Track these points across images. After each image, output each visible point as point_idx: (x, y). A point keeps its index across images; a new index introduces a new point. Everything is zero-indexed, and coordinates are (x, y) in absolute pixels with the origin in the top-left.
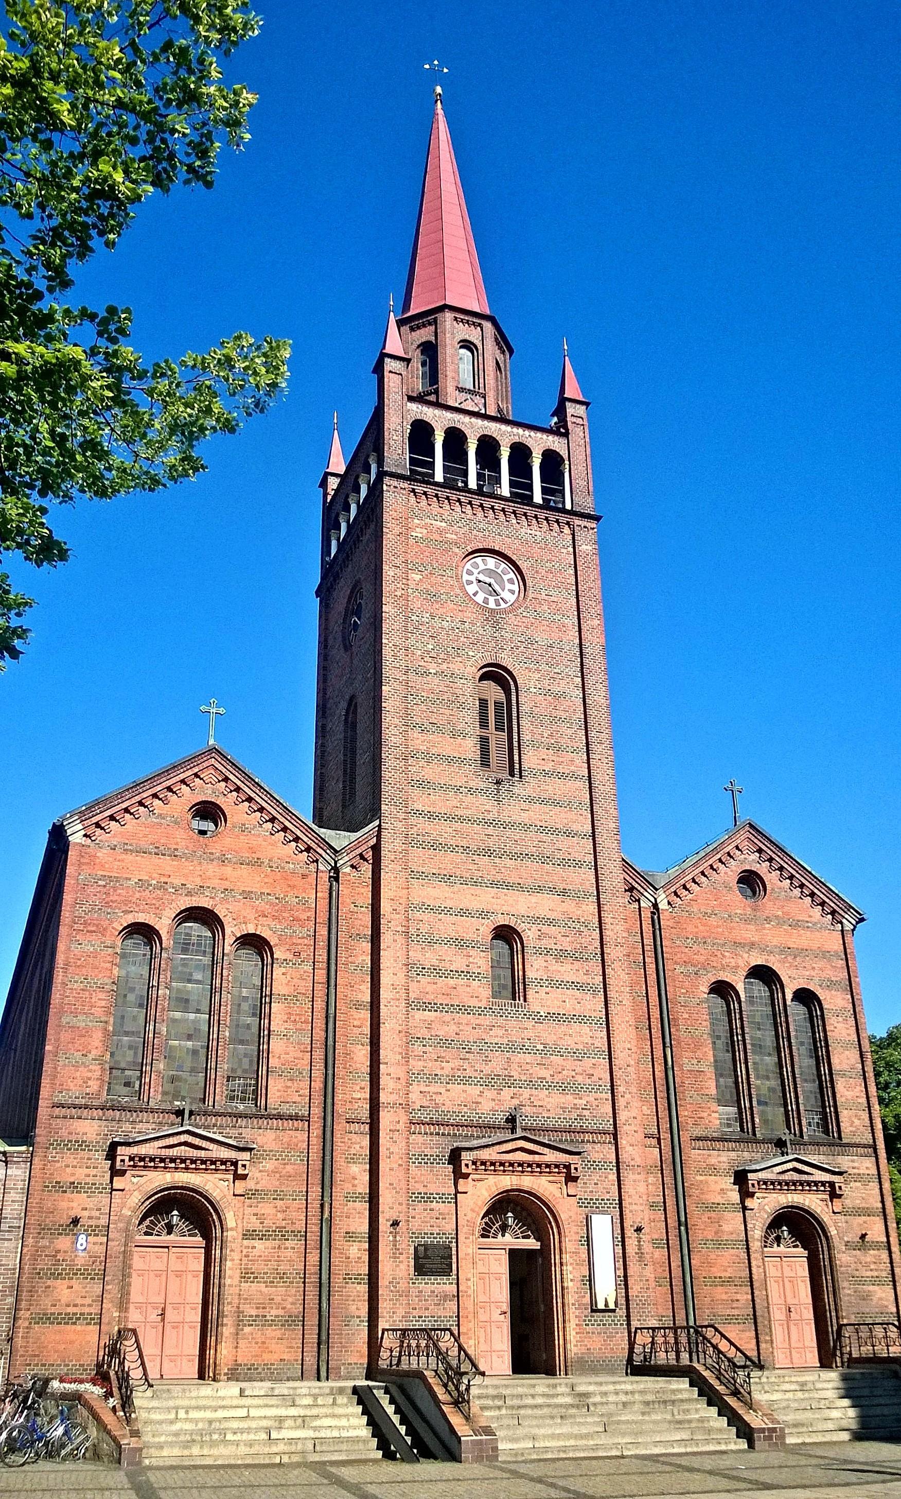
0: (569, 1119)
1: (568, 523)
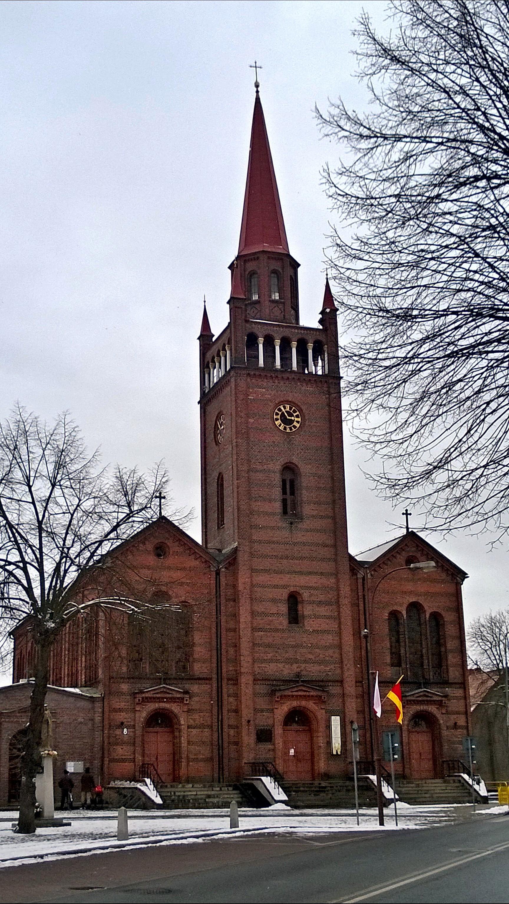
0: (323, 676)
1: (326, 382)
